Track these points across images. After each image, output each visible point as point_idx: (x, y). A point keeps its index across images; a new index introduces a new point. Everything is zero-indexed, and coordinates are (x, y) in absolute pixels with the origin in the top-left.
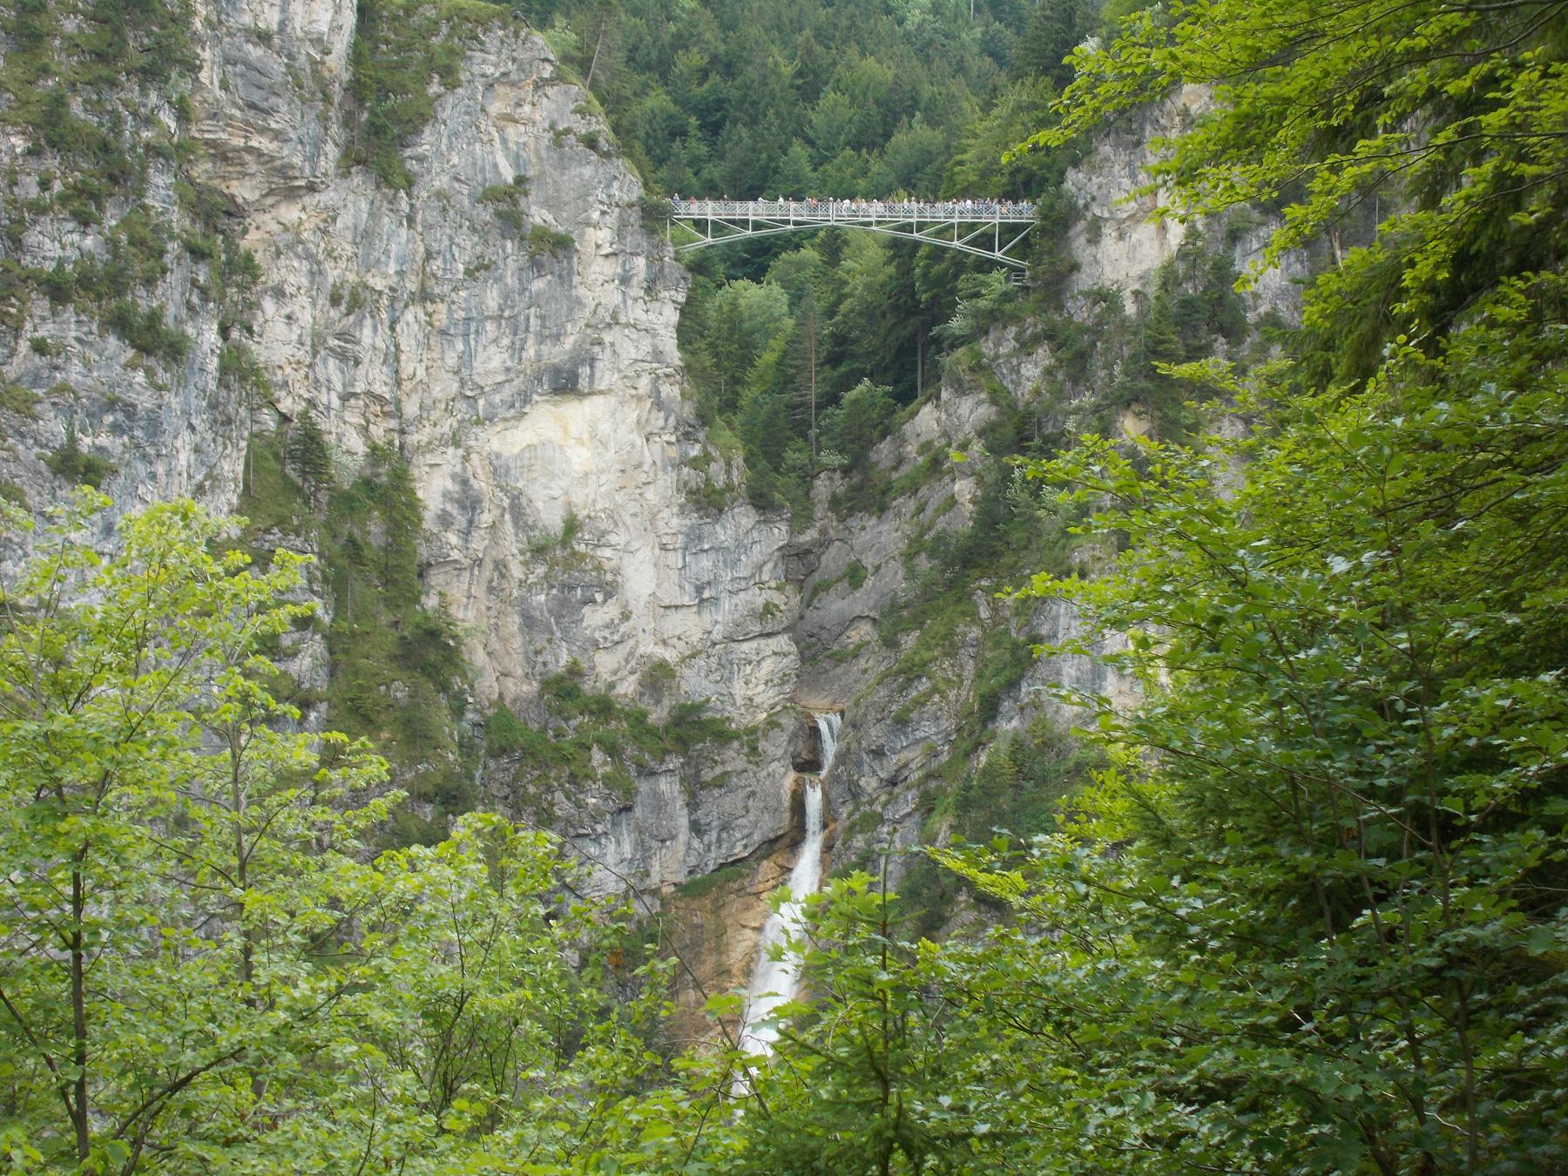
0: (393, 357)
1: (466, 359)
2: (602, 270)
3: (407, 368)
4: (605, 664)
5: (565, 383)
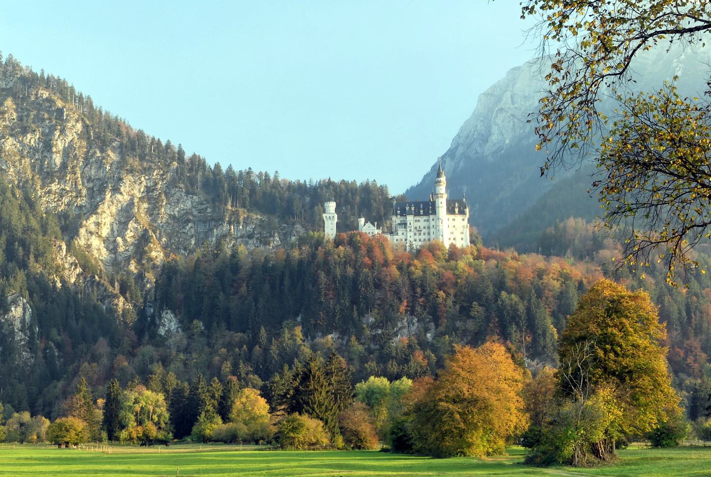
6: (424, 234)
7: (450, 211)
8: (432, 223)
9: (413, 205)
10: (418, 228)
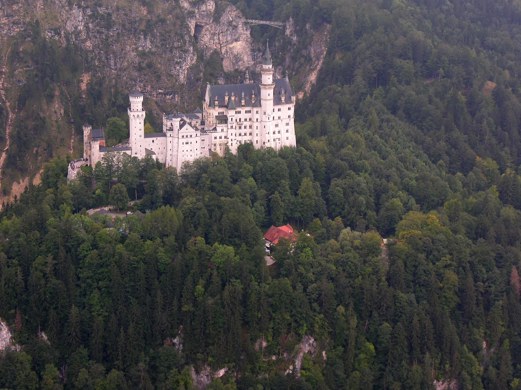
0: (219, 39)
1: (227, 38)
2: (240, 28)
3: (220, 39)
4: (241, 67)
5: (236, 40)
6: (245, 127)
7: (277, 101)
8: (257, 116)
9: (233, 94)
10: (238, 121)
